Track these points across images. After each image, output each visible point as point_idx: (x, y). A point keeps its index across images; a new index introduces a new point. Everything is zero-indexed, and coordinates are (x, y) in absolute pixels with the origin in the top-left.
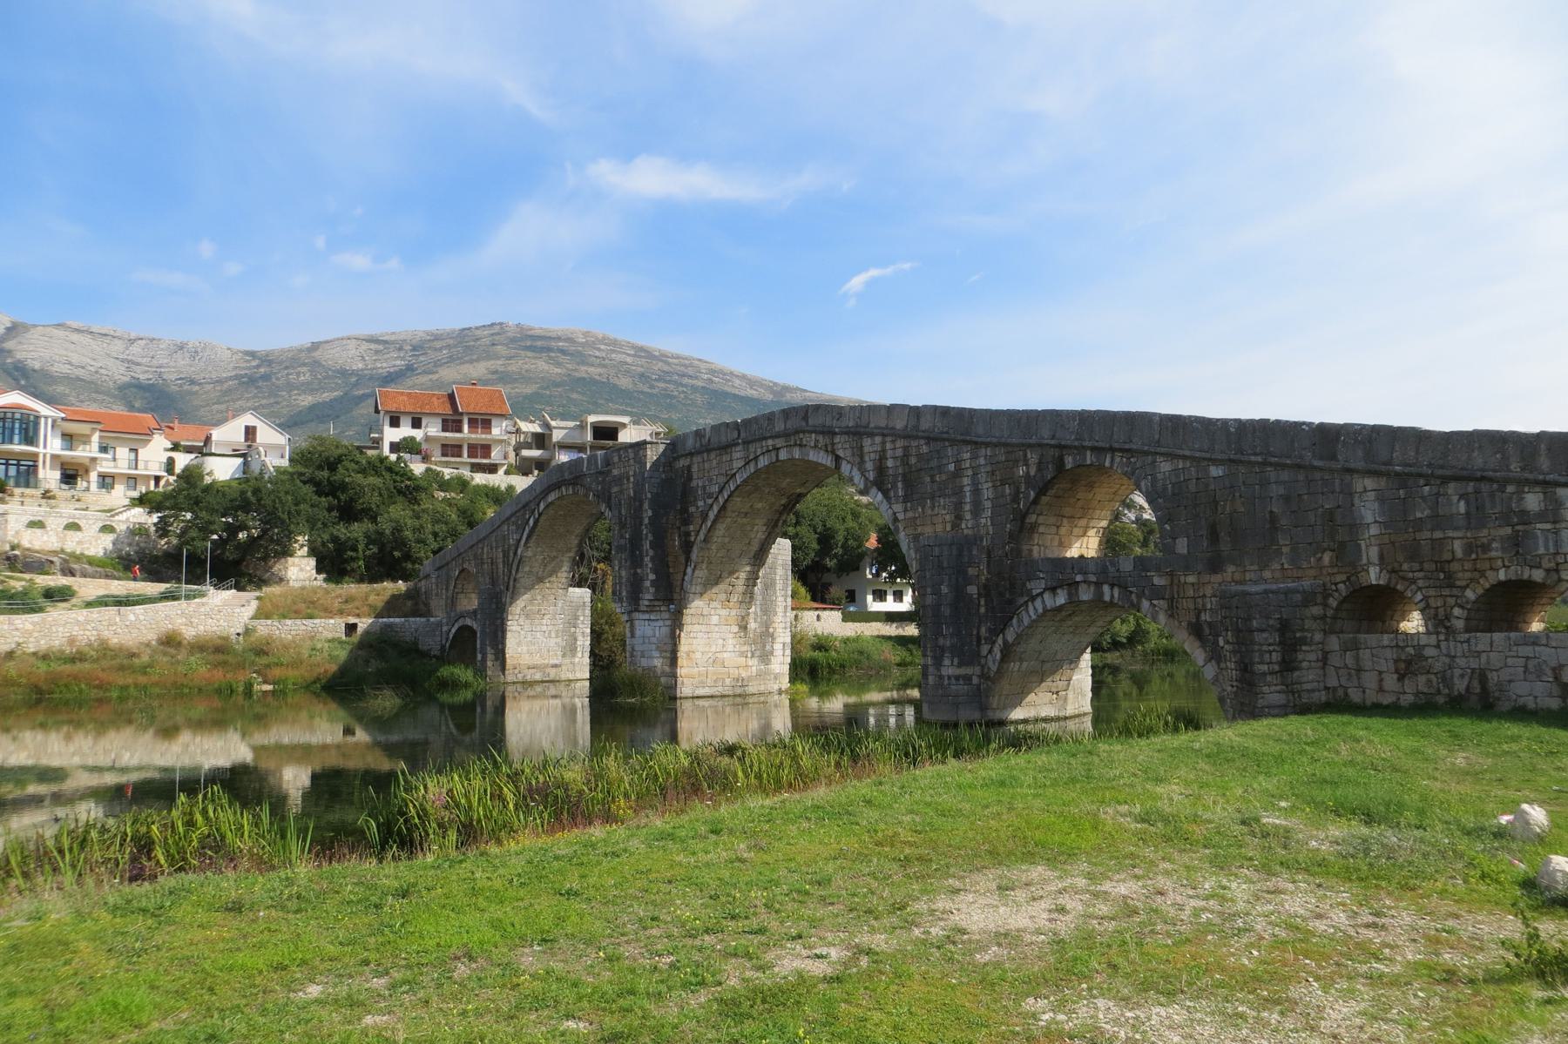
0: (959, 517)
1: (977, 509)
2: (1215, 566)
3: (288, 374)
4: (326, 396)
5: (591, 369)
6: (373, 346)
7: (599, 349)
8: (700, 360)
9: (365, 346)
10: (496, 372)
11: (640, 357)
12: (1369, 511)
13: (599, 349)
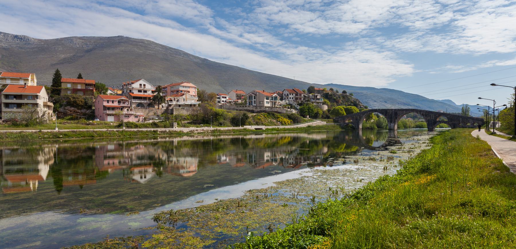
0: (431, 117)
1: (433, 117)
2: (451, 122)
3: (55, 48)
4: (68, 55)
5: (150, 52)
6: (81, 40)
7: (152, 46)
8: (181, 51)
9: (79, 40)
10: (122, 51)
11: (163, 49)
12: (461, 120)
13: (152, 46)
